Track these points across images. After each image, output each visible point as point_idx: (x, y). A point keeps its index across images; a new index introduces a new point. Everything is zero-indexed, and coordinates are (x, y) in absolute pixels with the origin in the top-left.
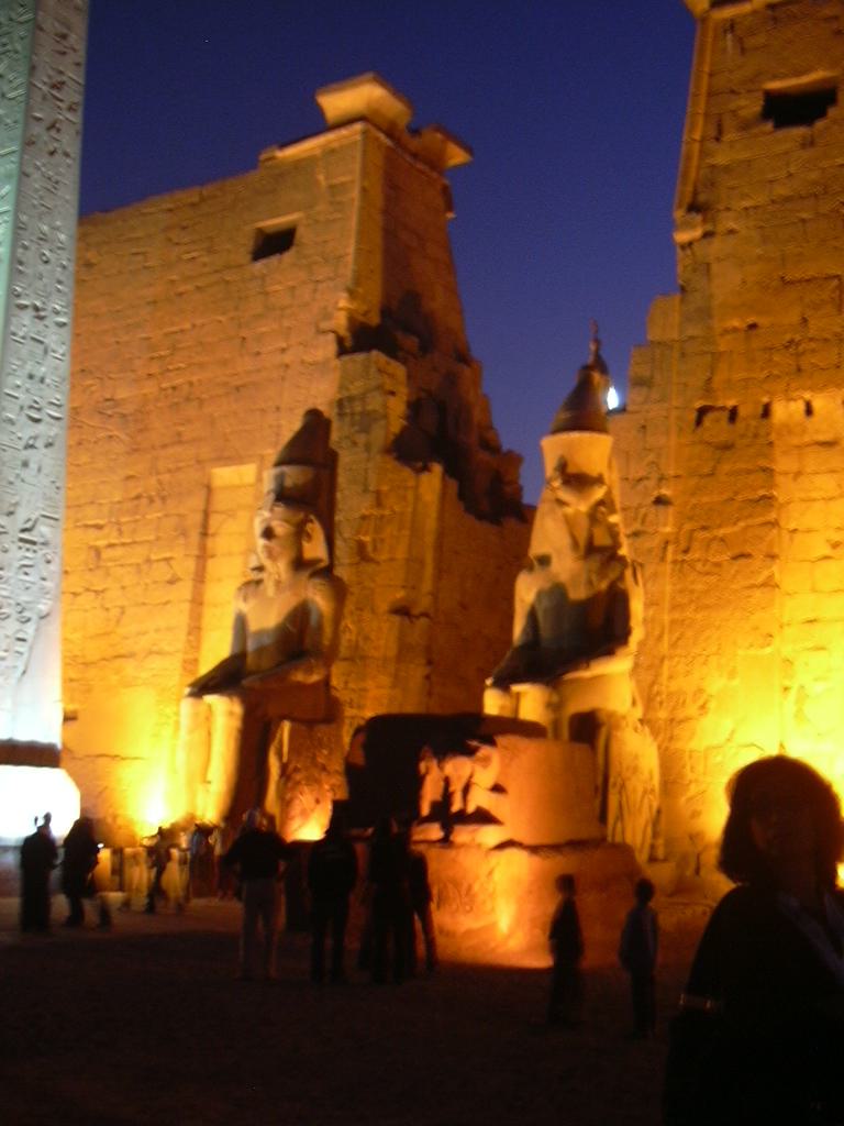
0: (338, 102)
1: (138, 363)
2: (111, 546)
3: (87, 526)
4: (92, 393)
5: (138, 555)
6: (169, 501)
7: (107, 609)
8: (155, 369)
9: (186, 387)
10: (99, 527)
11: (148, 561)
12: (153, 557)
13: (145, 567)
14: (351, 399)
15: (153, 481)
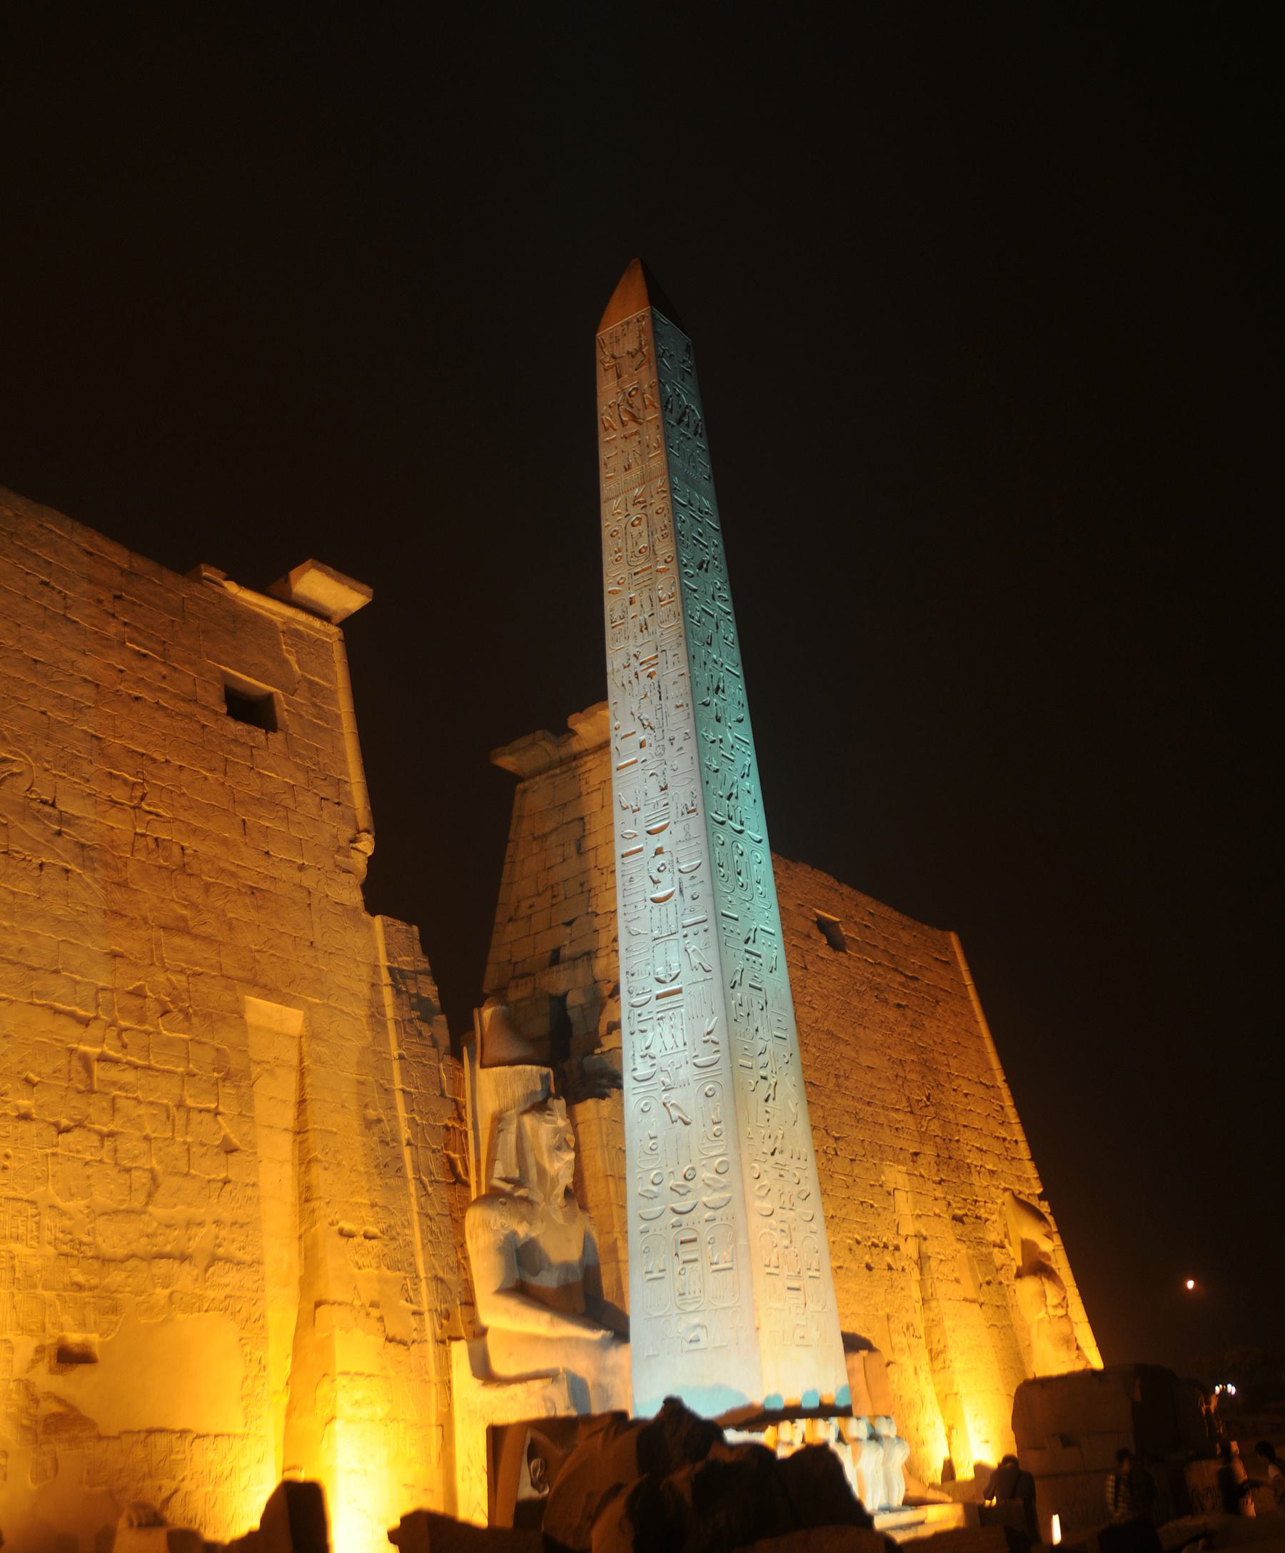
0: (316, 584)
1: (88, 769)
2: (103, 1059)
3: (58, 1012)
4: (12, 775)
5: (165, 1092)
6: (195, 1020)
7: (128, 1170)
8: (119, 794)
9: (176, 850)
10: (86, 1022)
11: (180, 1105)
12: (190, 1102)
13: (180, 1117)
14: (401, 971)
15: (161, 978)
